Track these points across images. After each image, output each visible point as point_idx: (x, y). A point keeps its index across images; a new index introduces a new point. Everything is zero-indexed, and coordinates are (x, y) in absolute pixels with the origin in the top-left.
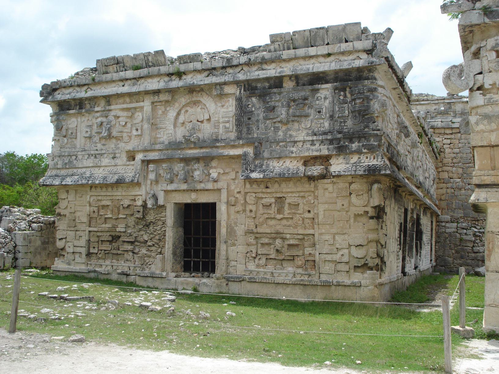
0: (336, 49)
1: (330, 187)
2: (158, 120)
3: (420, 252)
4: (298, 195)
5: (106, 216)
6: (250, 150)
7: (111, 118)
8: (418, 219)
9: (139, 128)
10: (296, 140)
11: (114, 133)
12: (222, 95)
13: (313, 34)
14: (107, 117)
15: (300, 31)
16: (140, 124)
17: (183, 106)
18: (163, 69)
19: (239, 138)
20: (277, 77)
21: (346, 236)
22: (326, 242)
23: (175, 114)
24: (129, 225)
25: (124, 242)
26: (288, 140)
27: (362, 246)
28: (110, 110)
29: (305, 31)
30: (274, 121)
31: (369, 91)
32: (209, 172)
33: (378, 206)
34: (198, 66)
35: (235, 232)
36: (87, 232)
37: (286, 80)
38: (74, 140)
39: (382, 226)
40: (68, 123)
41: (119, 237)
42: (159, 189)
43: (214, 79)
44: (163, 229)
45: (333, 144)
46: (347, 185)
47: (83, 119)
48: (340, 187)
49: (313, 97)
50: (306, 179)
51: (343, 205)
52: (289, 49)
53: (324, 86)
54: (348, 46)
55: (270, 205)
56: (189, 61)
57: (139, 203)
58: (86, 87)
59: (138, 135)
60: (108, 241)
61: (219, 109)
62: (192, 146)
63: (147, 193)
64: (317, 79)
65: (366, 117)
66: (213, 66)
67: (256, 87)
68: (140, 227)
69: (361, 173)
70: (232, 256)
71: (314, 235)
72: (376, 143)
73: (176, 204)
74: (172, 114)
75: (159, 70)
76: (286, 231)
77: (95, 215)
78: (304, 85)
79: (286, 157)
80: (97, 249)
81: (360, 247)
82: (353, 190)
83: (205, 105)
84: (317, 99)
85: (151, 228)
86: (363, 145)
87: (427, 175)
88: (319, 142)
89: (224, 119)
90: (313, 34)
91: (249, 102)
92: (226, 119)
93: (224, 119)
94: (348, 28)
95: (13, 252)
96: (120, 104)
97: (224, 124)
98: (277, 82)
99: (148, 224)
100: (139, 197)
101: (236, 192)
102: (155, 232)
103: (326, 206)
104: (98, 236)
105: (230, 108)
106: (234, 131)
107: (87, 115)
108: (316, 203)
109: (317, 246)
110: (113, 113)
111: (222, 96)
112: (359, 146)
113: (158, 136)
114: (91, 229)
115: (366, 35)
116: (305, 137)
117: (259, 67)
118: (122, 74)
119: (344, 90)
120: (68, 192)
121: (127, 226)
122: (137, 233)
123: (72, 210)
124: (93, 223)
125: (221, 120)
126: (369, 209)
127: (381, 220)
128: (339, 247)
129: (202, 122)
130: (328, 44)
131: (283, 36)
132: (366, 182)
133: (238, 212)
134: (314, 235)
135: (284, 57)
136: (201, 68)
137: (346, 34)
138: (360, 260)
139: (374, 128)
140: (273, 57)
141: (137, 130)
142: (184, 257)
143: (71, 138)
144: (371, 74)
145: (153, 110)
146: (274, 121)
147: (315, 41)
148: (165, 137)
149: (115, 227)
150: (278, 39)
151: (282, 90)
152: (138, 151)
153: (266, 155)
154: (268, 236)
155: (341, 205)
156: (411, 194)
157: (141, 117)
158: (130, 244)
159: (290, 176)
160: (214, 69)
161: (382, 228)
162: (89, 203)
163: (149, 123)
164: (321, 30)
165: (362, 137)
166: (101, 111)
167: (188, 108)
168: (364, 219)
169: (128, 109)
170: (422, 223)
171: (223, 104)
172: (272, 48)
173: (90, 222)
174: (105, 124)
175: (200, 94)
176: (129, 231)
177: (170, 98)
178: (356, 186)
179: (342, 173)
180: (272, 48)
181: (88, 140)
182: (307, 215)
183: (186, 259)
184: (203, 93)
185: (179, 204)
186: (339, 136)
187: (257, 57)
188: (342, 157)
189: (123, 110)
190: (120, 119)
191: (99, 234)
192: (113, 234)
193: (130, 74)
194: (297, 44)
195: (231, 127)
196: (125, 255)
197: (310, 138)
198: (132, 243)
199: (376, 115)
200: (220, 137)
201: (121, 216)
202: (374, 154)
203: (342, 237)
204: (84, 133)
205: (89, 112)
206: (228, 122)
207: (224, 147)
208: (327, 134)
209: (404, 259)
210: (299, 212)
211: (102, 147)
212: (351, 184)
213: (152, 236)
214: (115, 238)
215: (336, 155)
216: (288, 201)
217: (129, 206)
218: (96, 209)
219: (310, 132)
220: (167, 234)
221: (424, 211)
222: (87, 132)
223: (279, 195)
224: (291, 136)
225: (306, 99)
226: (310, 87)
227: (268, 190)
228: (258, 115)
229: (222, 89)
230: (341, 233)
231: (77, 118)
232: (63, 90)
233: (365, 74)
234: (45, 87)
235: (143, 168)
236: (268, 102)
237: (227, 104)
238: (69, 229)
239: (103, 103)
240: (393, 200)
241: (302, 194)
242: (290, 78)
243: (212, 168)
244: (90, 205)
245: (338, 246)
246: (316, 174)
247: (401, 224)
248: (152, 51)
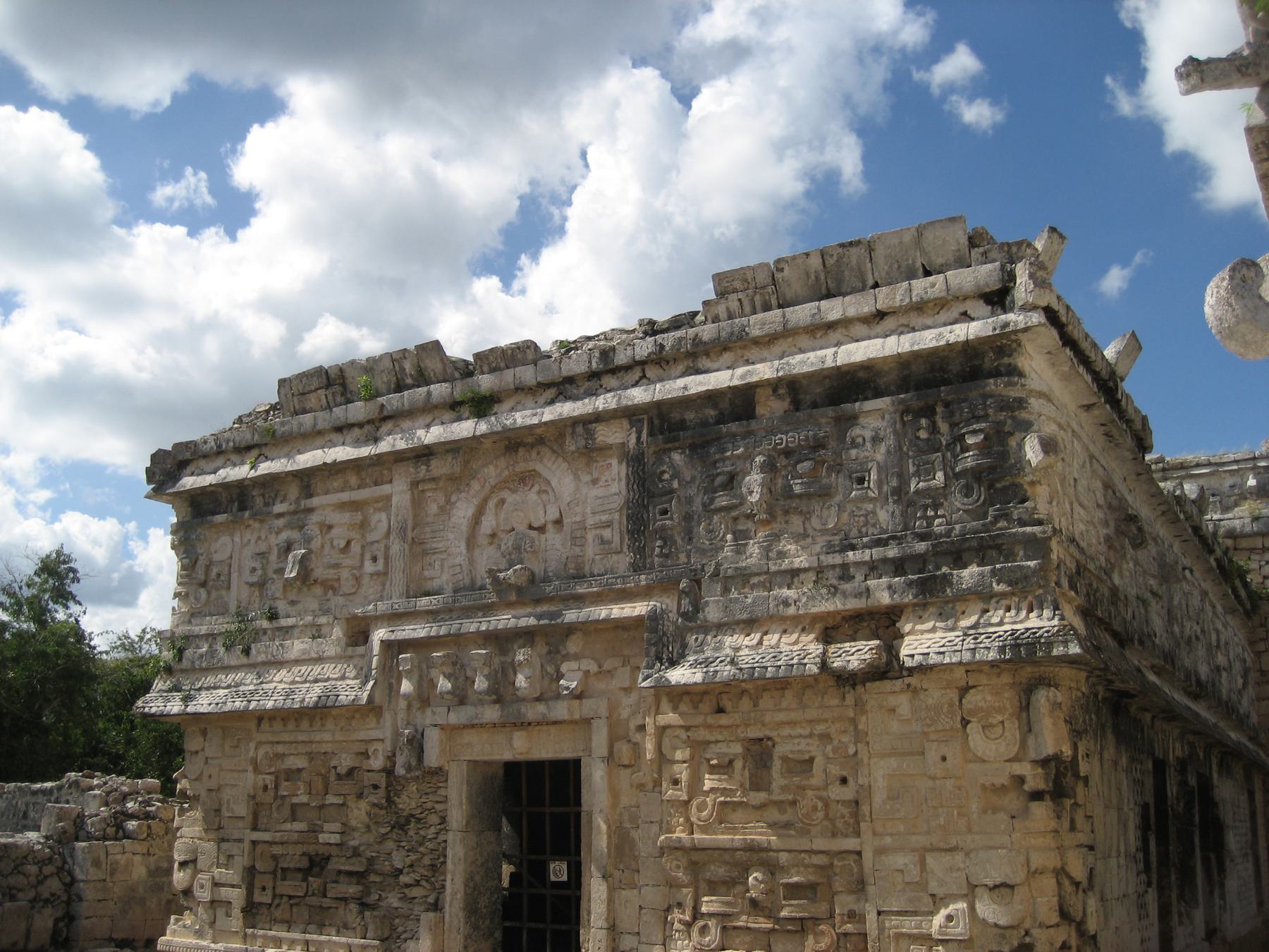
0: (898, 298)
1: (903, 703)
2: (428, 529)
3: (1222, 885)
4: (806, 732)
5: (295, 800)
6: (667, 603)
7: (312, 529)
8: (1205, 786)
10: (796, 566)
11: (319, 572)
12: (591, 450)
13: (831, 261)
14: (301, 528)
15: (794, 258)
16: (382, 545)
17: (494, 489)
18: (439, 390)
19: (636, 568)
20: (736, 387)
21: (959, 857)
22: (899, 878)
23: (470, 512)
24: (353, 823)
25: (340, 872)
26: (773, 568)
27: (1012, 887)
28: (310, 510)
29: (807, 255)
30: (734, 514)
31: (1002, 409)
32: (558, 671)
33: (1056, 758)
34: (527, 374)
35: (632, 844)
36: (247, 845)
37: (761, 394)
38: (224, 592)
39: (1072, 821)
40: (212, 550)
41: (328, 858)
42: (428, 722)
43: (567, 409)
44: (441, 838)
45: (904, 574)
46: (954, 694)
47: (248, 536)
48: (930, 701)
49: (842, 438)
50: (831, 682)
51: (944, 759)
52: (767, 308)
53: (870, 405)
54: (933, 285)
55: (731, 762)
56: (502, 365)
57: (377, 763)
58: (255, 452)
59: (377, 574)
60: (299, 870)
61: (585, 490)
62: (513, 597)
63: (397, 734)
64: (852, 385)
65: (998, 486)
66: (565, 373)
67: (683, 421)
68: (383, 831)
69: (992, 655)
70: (627, 919)
71: (859, 853)
72: (1032, 564)
73: (474, 763)
74: (463, 511)
75: (429, 393)
77: (268, 797)
78: (815, 405)
79: (771, 618)
80: (269, 892)
81: (1004, 891)
82: (971, 712)
83: (549, 483)
84: (854, 444)
85: (411, 833)
86: (993, 572)
87: (1221, 660)
88: (864, 570)
89: (597, 518)
90: (831, 261)
91: (662, 463)
92: (604, 518)
93: (597, 518)
94: (929, 235)
95: (64, 898)
96: (337, 491)
97: (598, 531)
98: (740, 403)
99: (402, 821)
101: (632, 726)
102: (421, 844)
103: (893, 762)
104: (275, 858)
105: (613, 481)
106: (625, 549)
107: (257, 525)
108: (863, 754)
109: (871, 890)
110: (314, 518)
111: (592, 453)
112: (982, 574)
113: (426, 573)
114: (257, 836)
115: (981, 250)
116: (822, 557)
117: (688, 368)
118: (338, 411)
119: (929, 412)
120: (204, 733)
121: (346, 830)
122: (376, 847)
123: (213, 784)
124: (263, 821)
125: (590, 521)
126: (1024, 769)
127: (1068, 802)
128: (940, 892)
129: (542, 529)
130: (876, 285)
131: (749, 276)
132: (1013, 685)
133: (641, 786)
134: (859, 853)
135: (755, 332)
136: (533, 382)
137: (924, 252)
138: (1008, 933)
139: (1025, 517)
140: (723, 334)
141: (375, 559)
142: (505, 917)
143: (217, 589)
144: (1006, 360)
145: (418, 503)
146: (734, 514)
147: (840, 281)
148: (445, 577)
149: (314, 830)
150: (737, 284)
151: (754, 425)
153: (713, 613)
154: (727, 857)
155: (938, 758)
156: (1170, 714)
157: (385, 525)
158: (354, 880)
159: (781, 673)
160: (570, 380)
161: (1073, 828)
162: (254, 762)
163: (404, 539)
164: (853, 250)
165: (991, 547)
166: (289, 513)
167: (505, 494)
168: (1012, 801)
169: (354, 506)
170: (1217, 799)
171: (595, 476)
172: (721, 310)
173: (256, 815)
175: (534, 454)
176: (352, 843)
177: (457, 469)
178: (979, 697)
179: (934, 659)
180: (721, 310)
182: (838, 793)
183: (507, 924)
184: (544, 450)
185: (487, 763)
186: (921, 547)
187: (680, 339)
188: (932, 610)
189: (342, 506)
190: (335, 531)
191: (277, 850)
192: (311, 849)
193: (358, 411)
194: (790, 294)
195: (617, 539)
196: (341, 911)
197: (837, 559)
198: (359, 876)
199: (1028, 479)
200: (587, 568)
201: (331, 799)
202: (1030, 598)
203: (947, 858)
206: (609, 524)
207: (598, 599)
208: (886, 545)
209: (1164, 913)
210: (814, 781)
212: (964, 690)
213: (413, 857)
214: (316, 864)
215: (915, 605)
216: (780, 750)
217: (351, 772)
218: (269, 779)
219: (836, 539)
220: (450, 853)
221: (1221, 765)
222: (254, 570)
223: (754, 733)
224: (782, 555)
225: (819, 445)
226: (830, 412)
227: (724, 720)
228: (690, 500)
229: (590, 435)
230: (942, 845)
231: (232, 535)
232: (202, 463)
233: (989, 362)
234: (158, 457)
235: (388, 664)
236: (716, 462)
237: (606, 475)
239: (293, 491)
240: (1110, 736)
241: (820, 728)
242: (775, 391)
243: (567, 657)
244: (256, 770)
245: (933, 887)
246: (854, 663)
247: (1145, 807)
248: (411, 347)
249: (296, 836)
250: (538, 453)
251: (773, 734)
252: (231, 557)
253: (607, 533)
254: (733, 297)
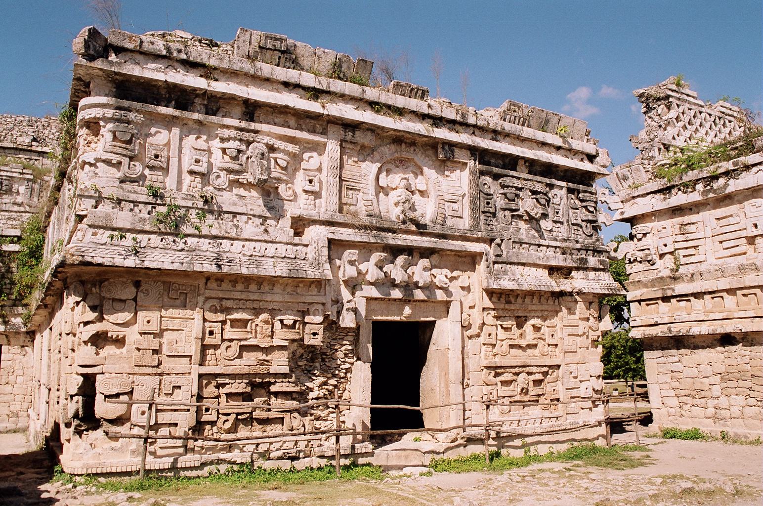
9: (316, 179)
59: (312, 192)
76: (533, 363)
92: (454, 197)
100: (316, 306)
114: (204, 370)
125: (447, 197)
152: (315, 222)
154: (513, 370)
169: (292, 140)
175: (412, 149)
196: (287, 420)
211: (236, 199)
218: (217, 328)
222: (197, 161)
226: (548, 181)
238: (137, 370)
249: (246, 370)
250: (414, 150)
251: (528, 315)
253: (455, 206)
254: (515, 114)
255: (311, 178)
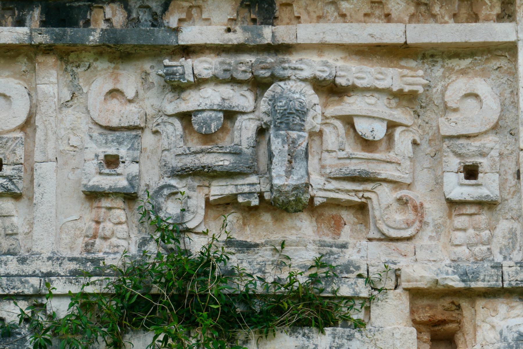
14: (259, 85)
107: (102, 65)
141: (471, 173)
174: (245, 130)
181: (120, 214)
190: (352, 105)
204: (92, 166)
205: (118, 51)
222: (112, 161)
252: (28, 125)
255: (470, 161)
